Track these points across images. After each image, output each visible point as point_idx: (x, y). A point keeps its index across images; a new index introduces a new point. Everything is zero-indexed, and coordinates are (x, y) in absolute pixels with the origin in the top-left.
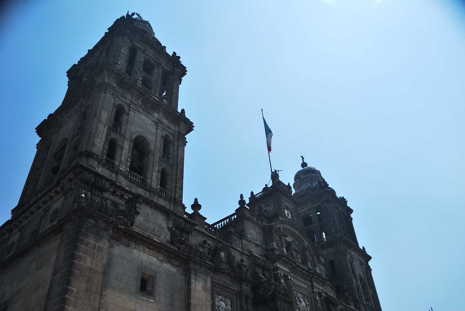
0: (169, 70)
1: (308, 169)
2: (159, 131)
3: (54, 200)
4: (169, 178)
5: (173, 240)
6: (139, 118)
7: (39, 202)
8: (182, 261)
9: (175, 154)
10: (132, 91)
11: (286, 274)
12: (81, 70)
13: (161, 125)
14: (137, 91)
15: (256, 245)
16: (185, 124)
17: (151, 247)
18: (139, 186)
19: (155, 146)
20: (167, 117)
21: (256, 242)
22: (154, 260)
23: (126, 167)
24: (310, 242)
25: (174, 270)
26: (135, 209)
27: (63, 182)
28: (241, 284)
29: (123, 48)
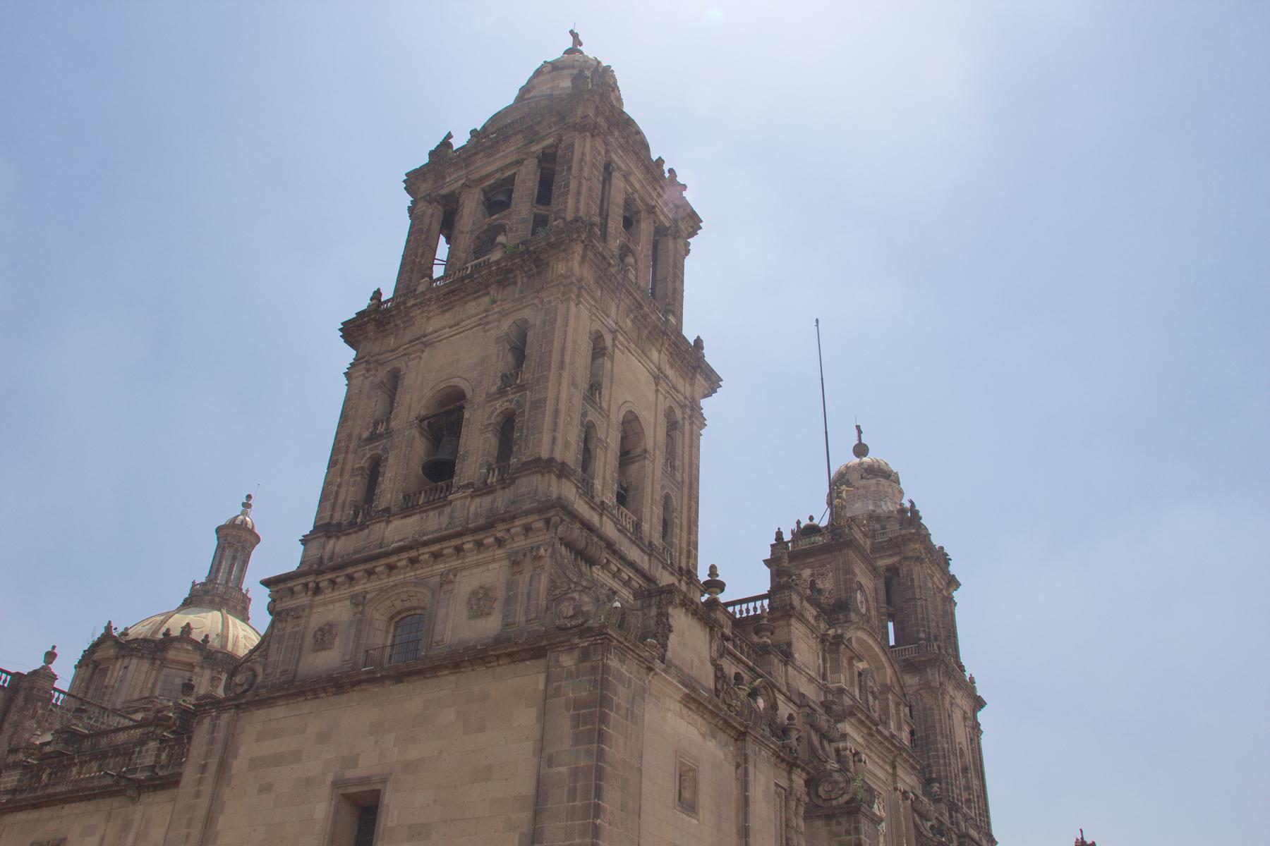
0: (667, 224)
1: (873, 465)
2: (661, 397)
3: (471, 559)
4: (676, 517)
5: (719, 687)
6: (627, 365)
7: (418, 551)
8: (732, 734)
9: (687, 456)
10: (618, 294)
11: (859, 750)
12: (448, 180)
13: (664, 385)
14: (630, 297)
15: (809, 680)
16: (705, 380)
17: (691, 706)
18: (634, 543)
19: (655, 437)
20: (674, 359)
21: (808, 671)
22: (695, 731)
23: (613, 496)
24: (896, 672)
25: (720, 754)
26: (667, 619)
27: (508, 530)
28: (790, 772)
29: (596, 172)
